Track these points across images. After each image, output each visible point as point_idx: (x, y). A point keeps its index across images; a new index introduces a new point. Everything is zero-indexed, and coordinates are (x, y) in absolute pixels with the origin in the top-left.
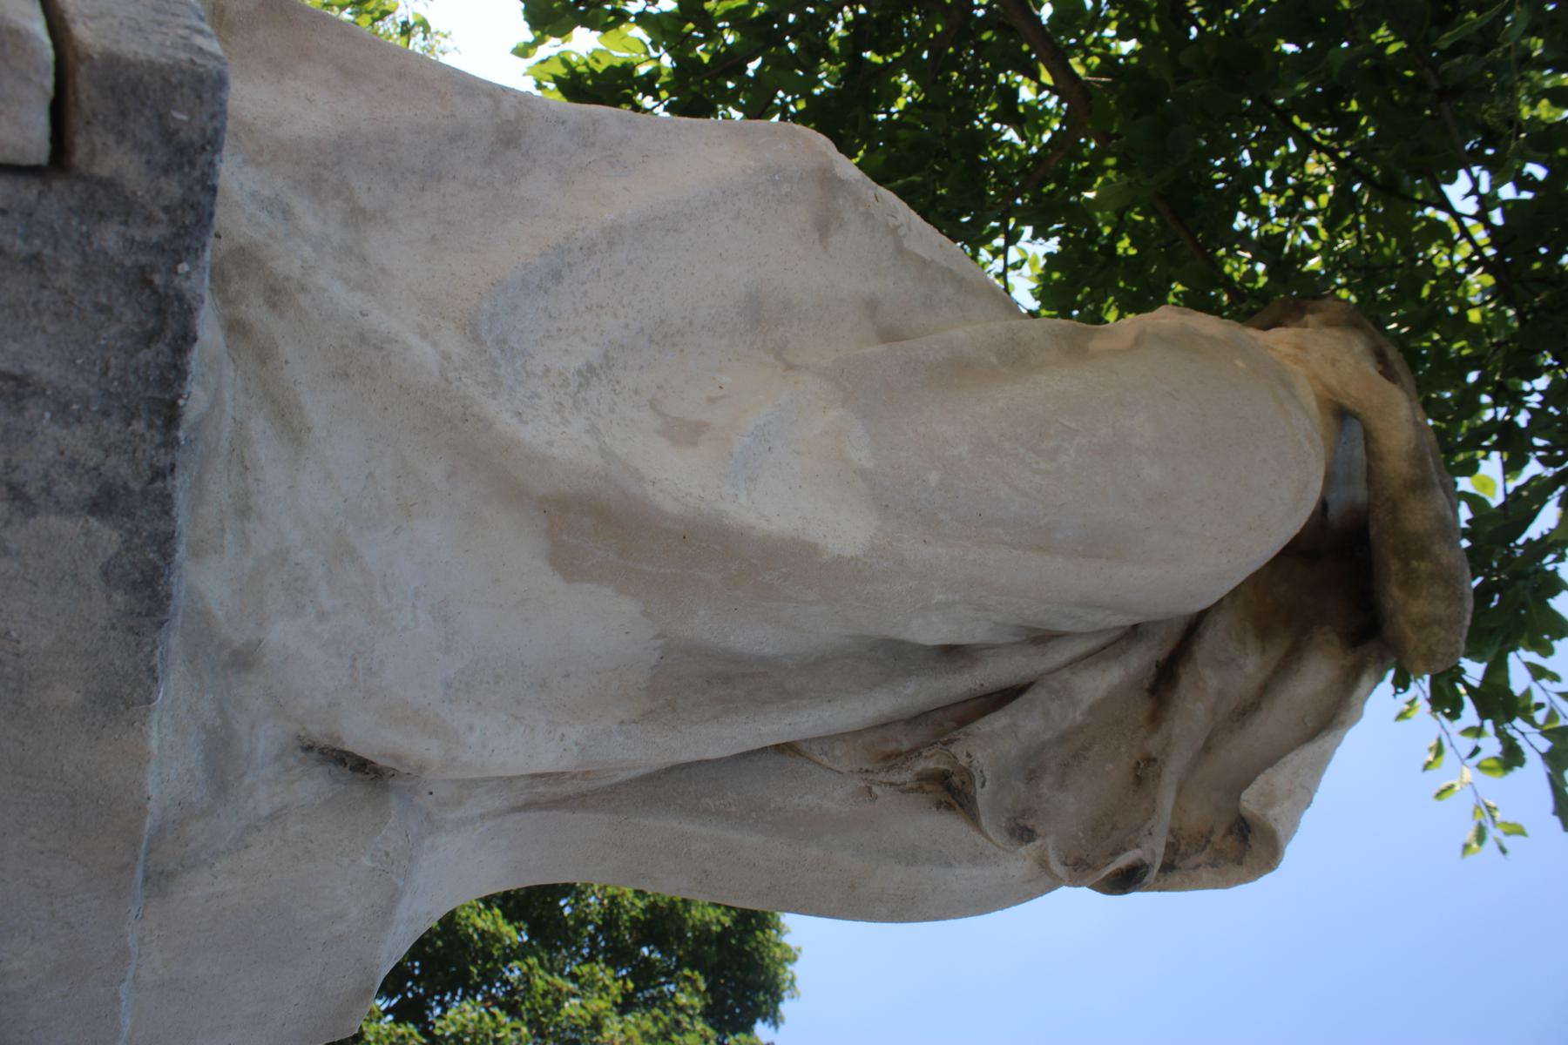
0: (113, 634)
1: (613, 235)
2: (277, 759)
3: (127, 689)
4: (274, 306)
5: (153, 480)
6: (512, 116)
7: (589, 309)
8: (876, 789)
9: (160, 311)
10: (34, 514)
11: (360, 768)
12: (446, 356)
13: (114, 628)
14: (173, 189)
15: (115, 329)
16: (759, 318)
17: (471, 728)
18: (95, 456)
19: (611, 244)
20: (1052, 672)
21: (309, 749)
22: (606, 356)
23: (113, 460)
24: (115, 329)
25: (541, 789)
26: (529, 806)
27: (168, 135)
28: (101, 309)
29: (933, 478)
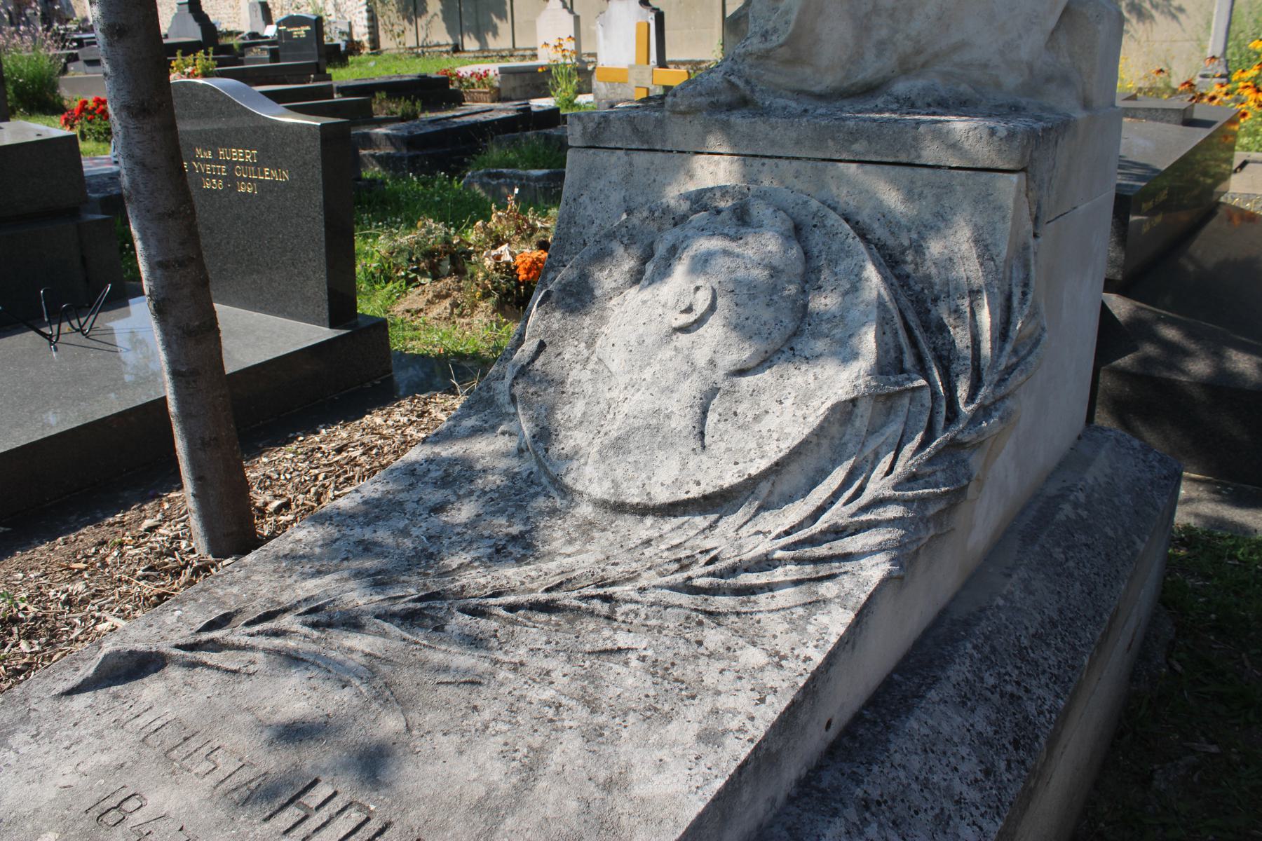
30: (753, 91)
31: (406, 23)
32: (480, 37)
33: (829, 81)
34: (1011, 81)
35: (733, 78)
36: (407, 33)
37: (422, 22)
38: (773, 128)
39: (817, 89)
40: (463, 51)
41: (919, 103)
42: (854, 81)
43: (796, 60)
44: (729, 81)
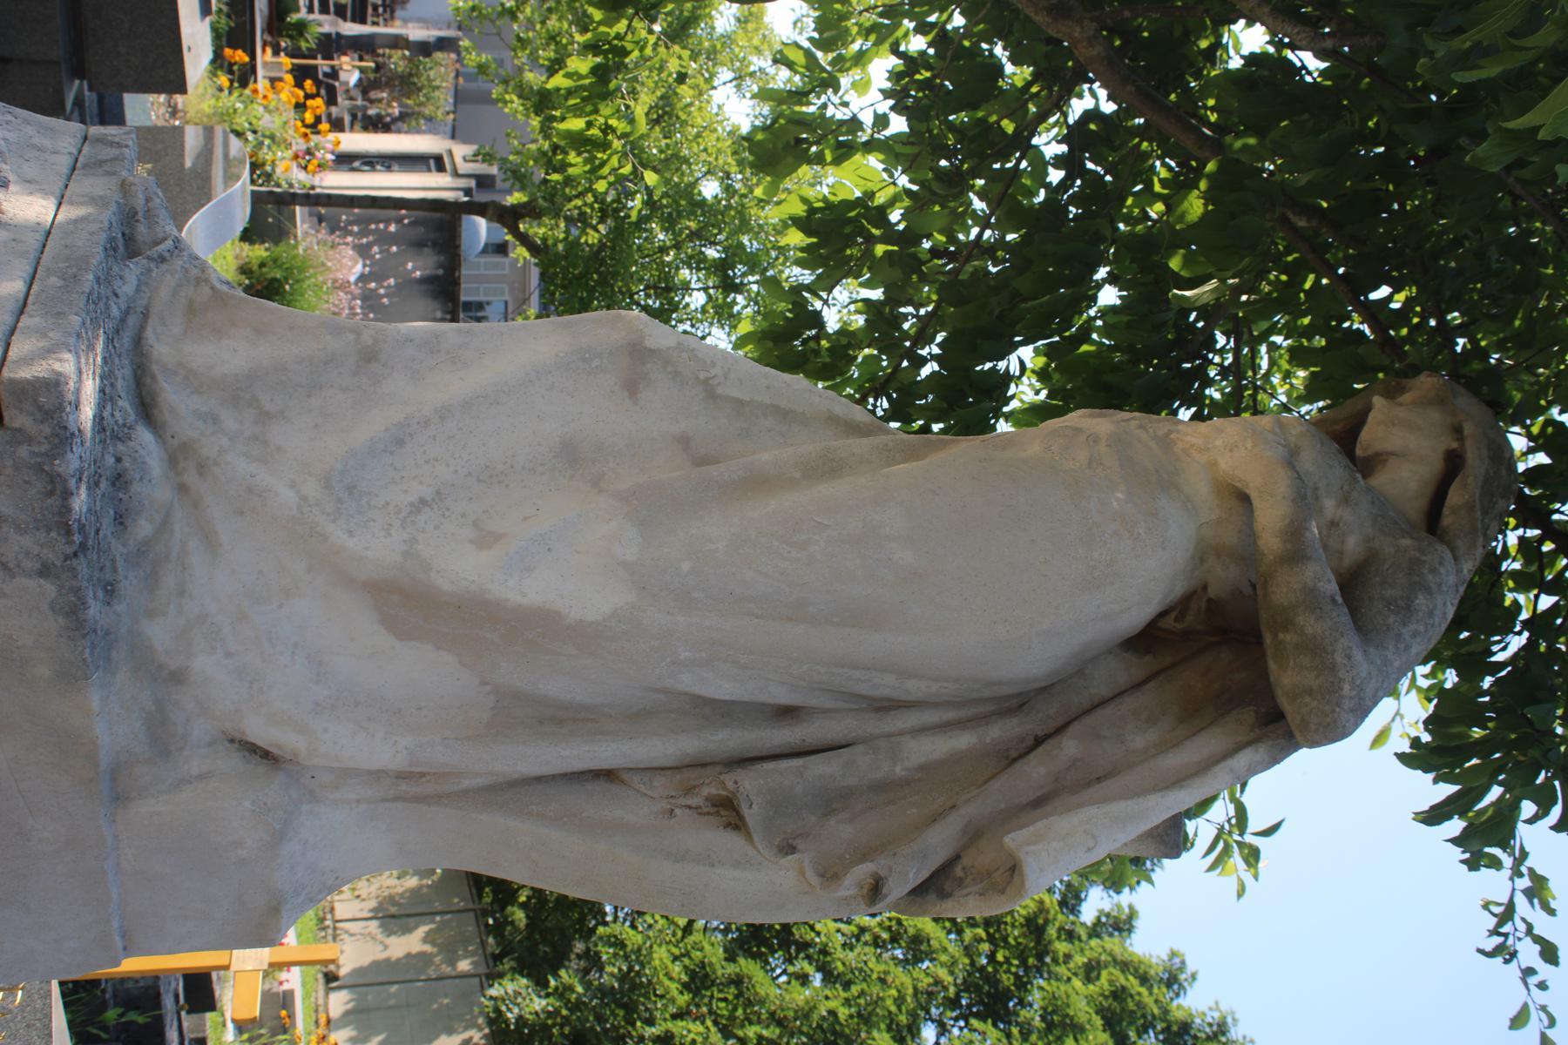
1: (444, 413)
2: (210, 745)
4: (201, 474)
6: (370, 342)
7: (427, 462)
8: (677, 811)
9: (52, 482)
10: (13, 576)
11: (266, 755)
12: (304, 498)
16: (573, 458)
17: (326, 730)
19: (442, 418)
20: (890, 735)
21: (232, 741)
22: (438, 493)
25: (404, 788)
26: (396, 799)
29: (686, 566)
30: (149, 258)
31: (373, 904)
32: (348, 1017)
33: (161, 348)
34: (158, 633)
35: (169, 244)
36: (357, 904)
37: (373, 925)
38: (92, 234)
39: (149, 334)
40: (328, 990)
41: (121, 447)
42: (160, 377)
43: (191, 310)
44: (165, 239)
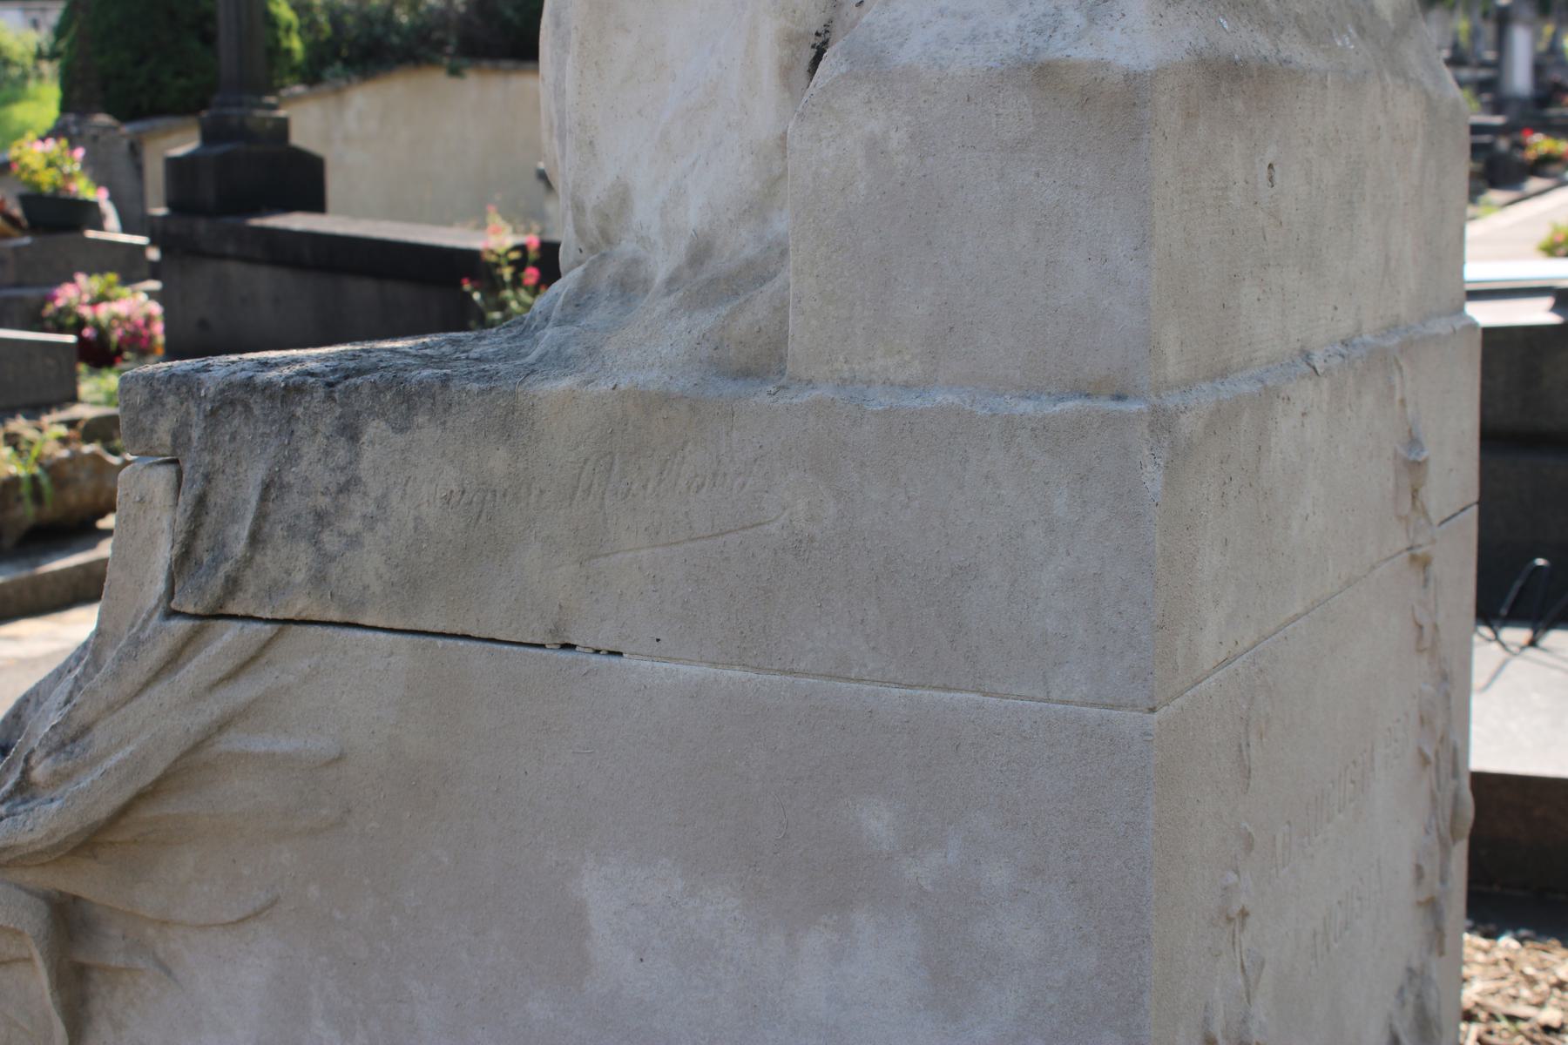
0: (449, 424)
3: (498, 412)
5: (334, 400)
9: (232, 403)
13: (444, 423)
14: (171, 400)
15: (245, 430)
18: (320, 439)
23: (321, 427)
24: (245, 430)
27: (148, 406)
28: (233, 438)
